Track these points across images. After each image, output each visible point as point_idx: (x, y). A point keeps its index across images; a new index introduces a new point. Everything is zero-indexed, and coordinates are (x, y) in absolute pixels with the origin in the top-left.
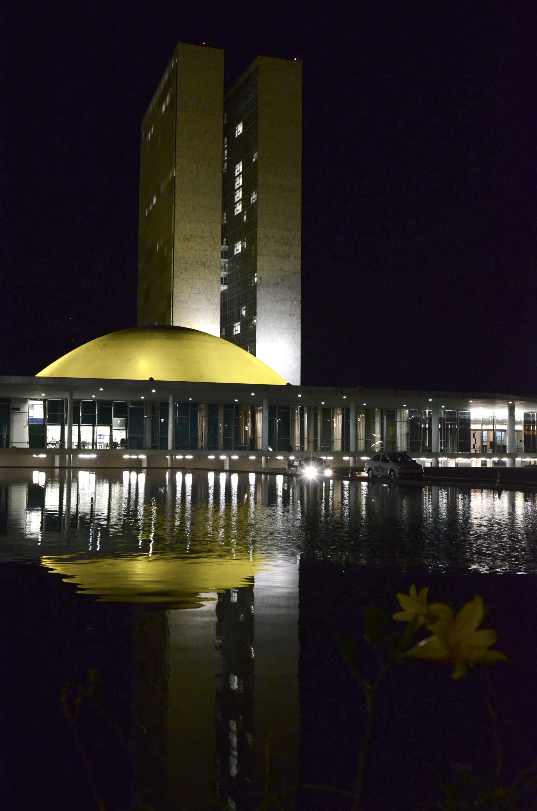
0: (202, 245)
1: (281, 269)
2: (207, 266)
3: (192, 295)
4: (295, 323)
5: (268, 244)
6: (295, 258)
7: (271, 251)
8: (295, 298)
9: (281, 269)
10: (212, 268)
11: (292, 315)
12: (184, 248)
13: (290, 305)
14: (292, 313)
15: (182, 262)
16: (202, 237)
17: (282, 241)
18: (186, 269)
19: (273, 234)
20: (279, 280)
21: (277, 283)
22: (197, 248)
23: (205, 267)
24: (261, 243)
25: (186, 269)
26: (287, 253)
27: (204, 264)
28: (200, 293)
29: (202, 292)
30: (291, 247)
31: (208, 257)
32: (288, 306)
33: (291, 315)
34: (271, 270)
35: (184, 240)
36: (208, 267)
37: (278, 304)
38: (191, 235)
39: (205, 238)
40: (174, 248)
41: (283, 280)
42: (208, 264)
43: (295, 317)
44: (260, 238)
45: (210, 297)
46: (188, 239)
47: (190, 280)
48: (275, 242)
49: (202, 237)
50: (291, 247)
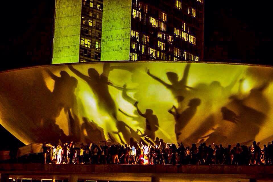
0: (68, 53)
5: (108, 42)
22: (65, 56)
24: (104, 42)
35: (59, 51)
38: (62, 47)
39: (71, 48)
48: (113, 40)
49: (69, 47)
50: (124, 41)
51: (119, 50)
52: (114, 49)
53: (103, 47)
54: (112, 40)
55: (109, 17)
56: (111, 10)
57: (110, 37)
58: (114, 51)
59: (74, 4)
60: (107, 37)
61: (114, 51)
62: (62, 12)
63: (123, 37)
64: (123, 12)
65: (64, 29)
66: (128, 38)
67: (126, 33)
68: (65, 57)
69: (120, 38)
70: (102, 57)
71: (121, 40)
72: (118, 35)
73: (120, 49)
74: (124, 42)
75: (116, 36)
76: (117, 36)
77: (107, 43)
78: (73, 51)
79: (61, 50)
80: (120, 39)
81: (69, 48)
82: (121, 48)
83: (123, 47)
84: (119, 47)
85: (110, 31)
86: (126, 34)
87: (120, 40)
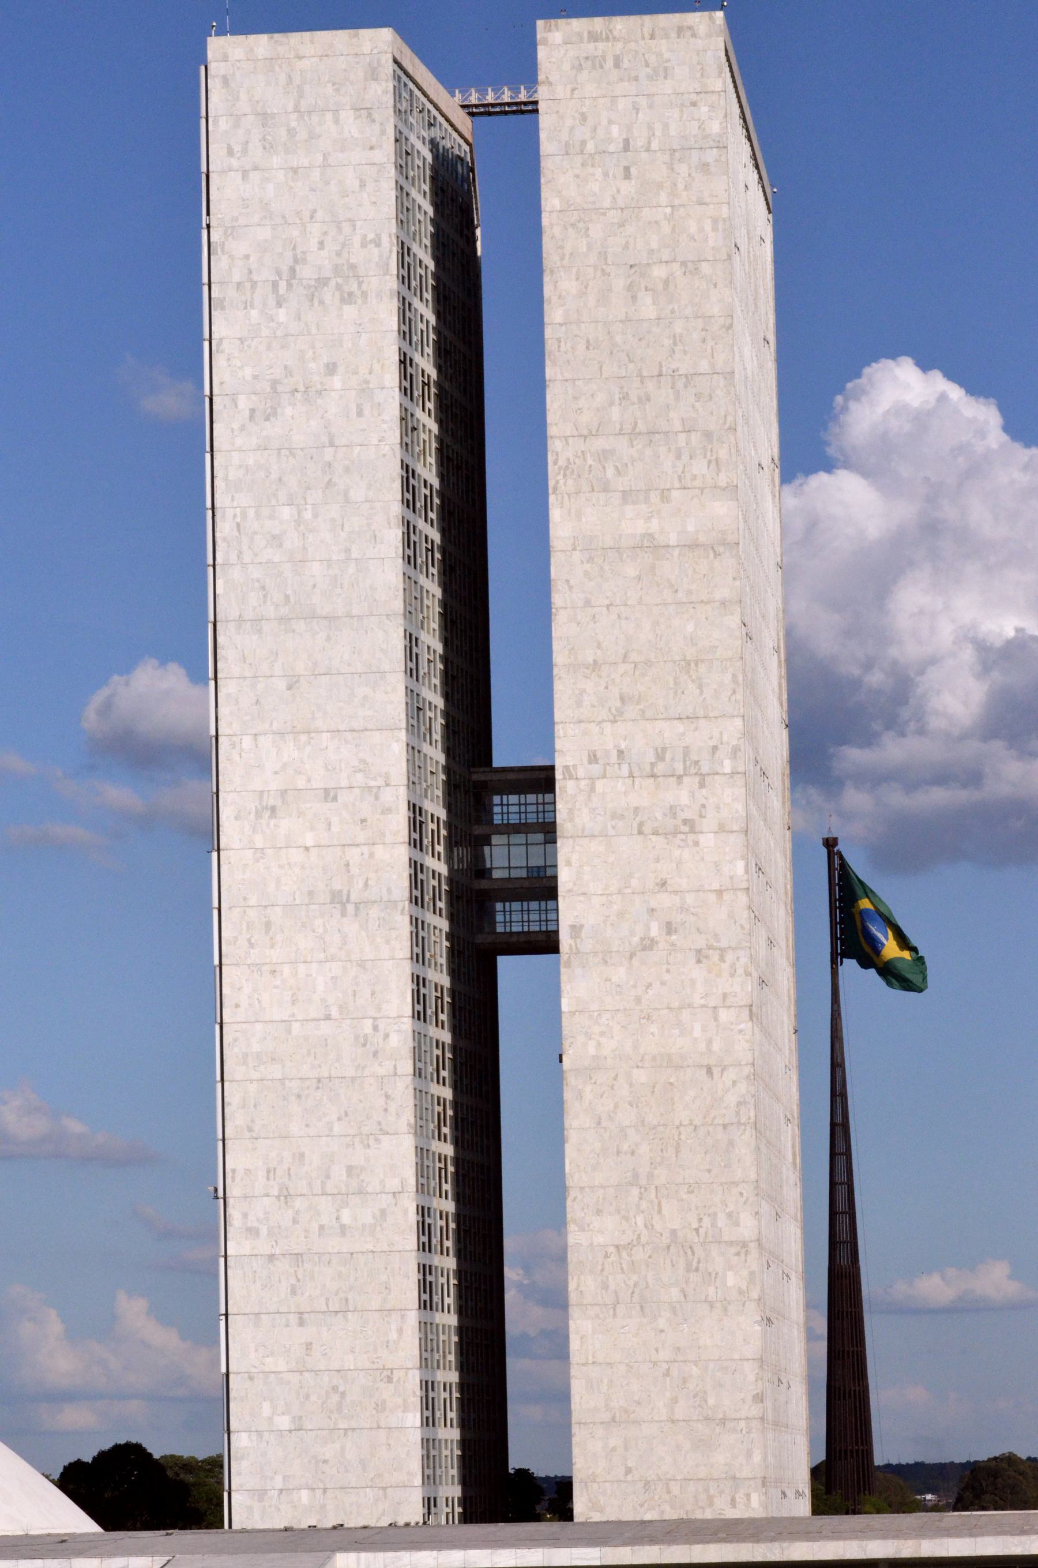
0: (329, 824)
1: (664, 884)
2: (351, 908)
3: (296, 1027)
4: (732, 1099)
5: (599, 785)
6: (722, 829)
7: (614, 816)
8: (725, 995)
9: (664, 884)
10: (374, 912)
11: (716, 1071)
12: (259, 842)
13: (704, 1029)
14: (712, 1062)
15: (253, 901)
16: (326, 791)
17: (660, 768)
18: (268, 925)
19: (623, 746)
20: (655, 931)
21: (648, 944)
23: (344, 914)
25: (268, 925)
26: (687, 815)
27: (339, 900)
28: (328, 1018)
29: (334, 1012)
30: (702, 785)
31: (355, 870)
32: (697, 1032)
33: (709, 1071)
34: (620, 892)
36: (357, 909)
37: (654, 1028)
38: (284, 793)
39: (343, 797)
40: (219, 850)
41: (670, 929)
42: (353, 897)
43: (731, 1074)
44: (567, 767)
45: (367, 1026)
46: (273, 809)
47: (286, 970)
48: (631, 776)
49: (329, 795)
50: (702, 785)
51: (675, 833)
52: (641, 825)
53: (571, 811)
54: (625, 768)
55: (599, 646)
56: (608, 607)
57: (614, 758)
58: (640, 832)
59: (348, 551)
60: (593, 758)
61: (640, 832)
62: (263, 588)
63: (697, 763)
64: (690, 628)
65: (289, 688)
66: (728, 770)
67: (711, 743)
68: (307, 849)
69: (679, 768)
70: (569, 863)
71: (686, 779)
72: (664, 750)
73: (686, 829)
74: (704, 791)
75: (651, 757)
76: (660, 755)
77: (592, 789)
78: (363, 821)
79: (273, 809)
80: (679, 768)
81: (335, 799)
82: (685, 822)
83: (701, 816)
84: (674, 816)
85: (608, 727)
86: (715, 748)
87: (680, 777)
